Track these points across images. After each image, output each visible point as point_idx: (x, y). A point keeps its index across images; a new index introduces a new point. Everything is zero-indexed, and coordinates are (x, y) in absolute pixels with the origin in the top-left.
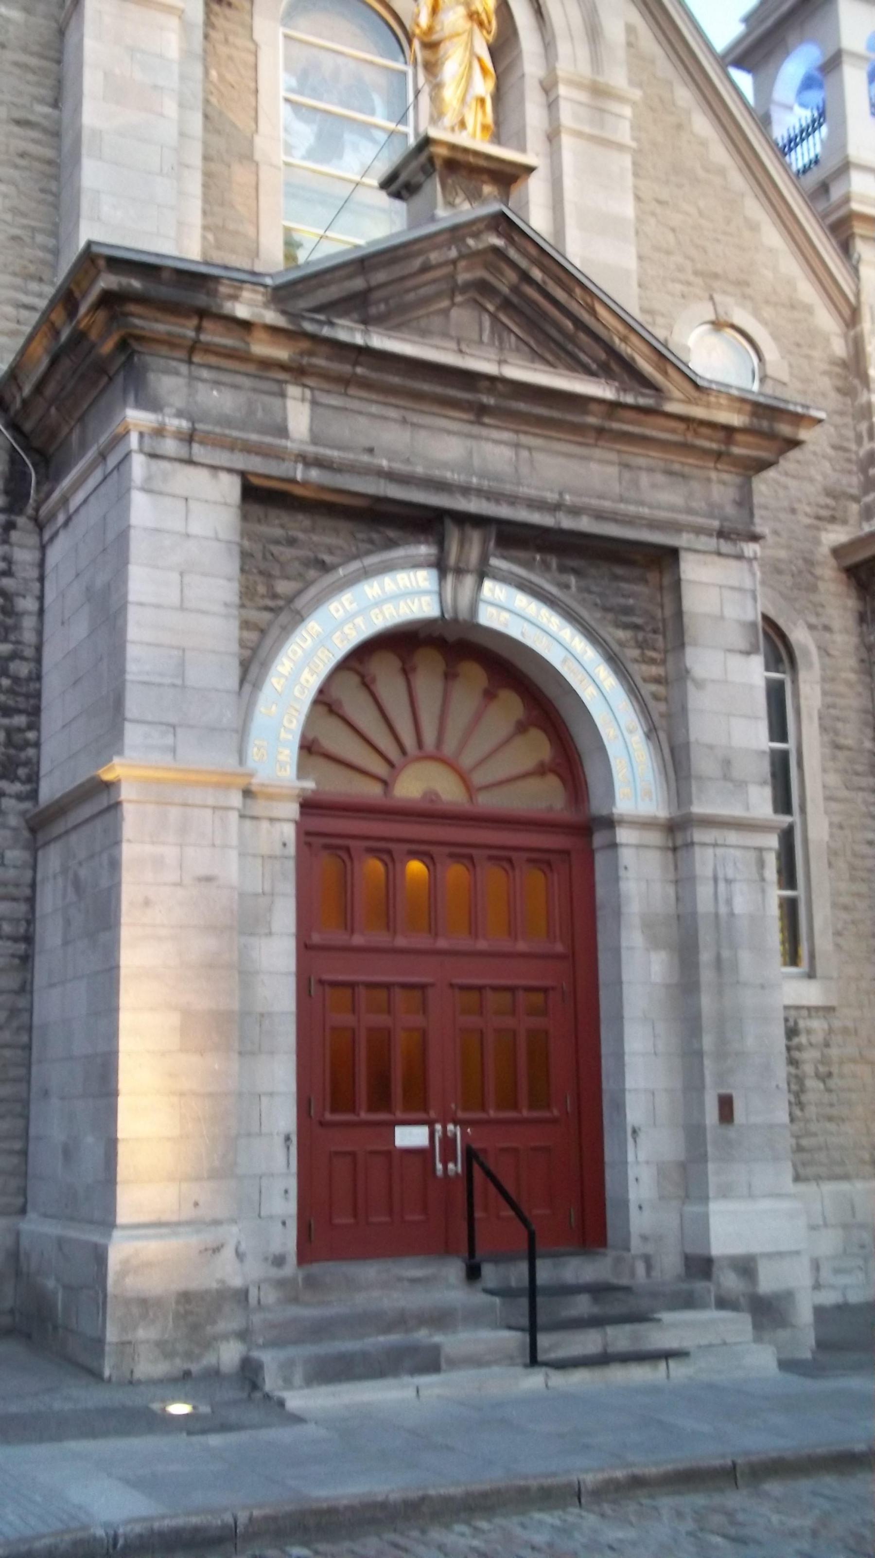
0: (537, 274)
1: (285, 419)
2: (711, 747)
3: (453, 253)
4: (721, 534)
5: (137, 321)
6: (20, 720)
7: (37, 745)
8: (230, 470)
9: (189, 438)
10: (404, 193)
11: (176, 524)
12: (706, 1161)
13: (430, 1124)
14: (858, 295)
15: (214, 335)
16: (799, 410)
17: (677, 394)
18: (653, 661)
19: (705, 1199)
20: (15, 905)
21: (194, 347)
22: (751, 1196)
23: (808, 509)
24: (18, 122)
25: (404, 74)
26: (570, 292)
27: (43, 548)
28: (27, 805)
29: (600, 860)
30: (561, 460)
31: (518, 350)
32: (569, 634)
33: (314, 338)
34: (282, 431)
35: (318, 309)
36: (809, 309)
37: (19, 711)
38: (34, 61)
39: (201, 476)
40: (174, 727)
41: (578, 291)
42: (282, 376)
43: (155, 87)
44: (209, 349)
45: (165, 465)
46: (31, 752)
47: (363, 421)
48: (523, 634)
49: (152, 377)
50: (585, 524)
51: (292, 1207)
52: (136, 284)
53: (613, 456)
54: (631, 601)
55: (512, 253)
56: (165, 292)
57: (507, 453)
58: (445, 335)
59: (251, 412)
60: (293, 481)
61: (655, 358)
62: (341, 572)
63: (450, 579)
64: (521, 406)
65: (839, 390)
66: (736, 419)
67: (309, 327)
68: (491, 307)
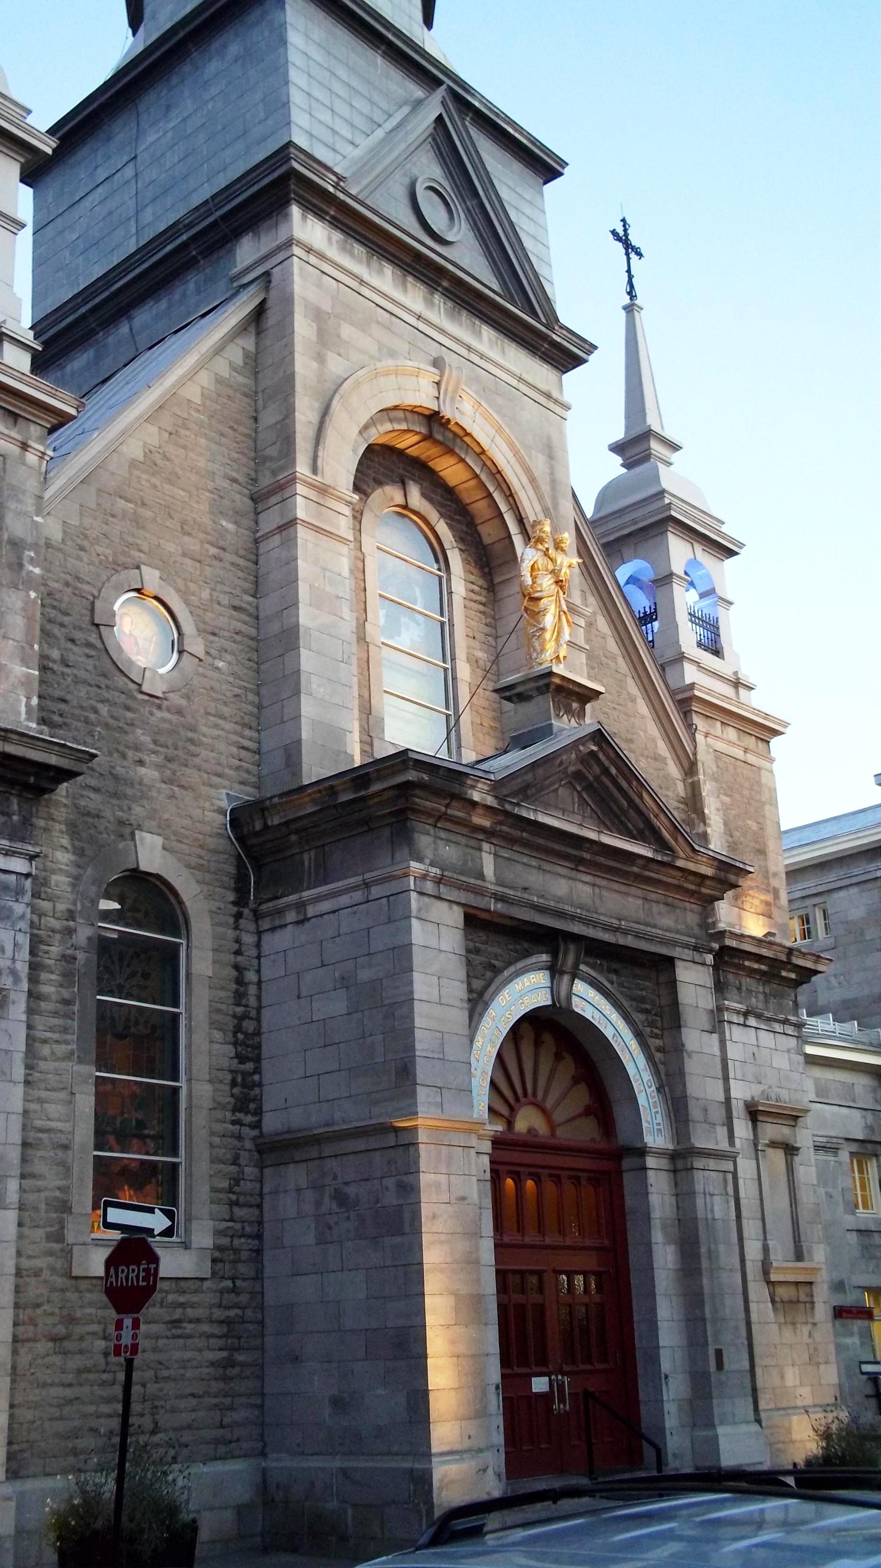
0: (613, 771)
2: (697, 1099)
4: (696, 949)
5: (417, 800)
6: (249, 1066)
7: (260, 1085)
8: (458, 904)
10: (515, 699)
11: (433, 943)
12: (712, 1398)
13: (548, 1374)
14: (695, 754)
15: (456, 812)
16: (741, 866)
17: (682, 854)
19: (712, 1426)
20: (251, 1210)
21: (442, 817)
22: (735, 1423)
24: (235, 608)
25: (440, 578)
26: (630, 784)
27: (259, 933)
28: (256, 1133)
29: (628, 1179)
30: (615, 896)
31: (591, 818)
32: (615, 1017)
33: (507, 814)
36: (664, 760)
37: (249, 1059)
38: (241, 562)
39: (443, 906)
40: (440, 1088)
41: (634, 783)
42: (481, 836)
43: (338, 597)
45: (426, 899)
46: (257, 1091)
47: (519, 867)
49: (416, 835)
50: (629, 941)
52: (426, 777)
53: (639, 892)
54: (644, 993)
55: (601, 756)
56: (439, 783)
57: (588, 889)
58: (557, 807)
59: (466, 862)
60: (488, 911)
61: (672, 829)
64: (601, 860)
66: (709, 871)
67: (508, 807)
68: (579, 788)
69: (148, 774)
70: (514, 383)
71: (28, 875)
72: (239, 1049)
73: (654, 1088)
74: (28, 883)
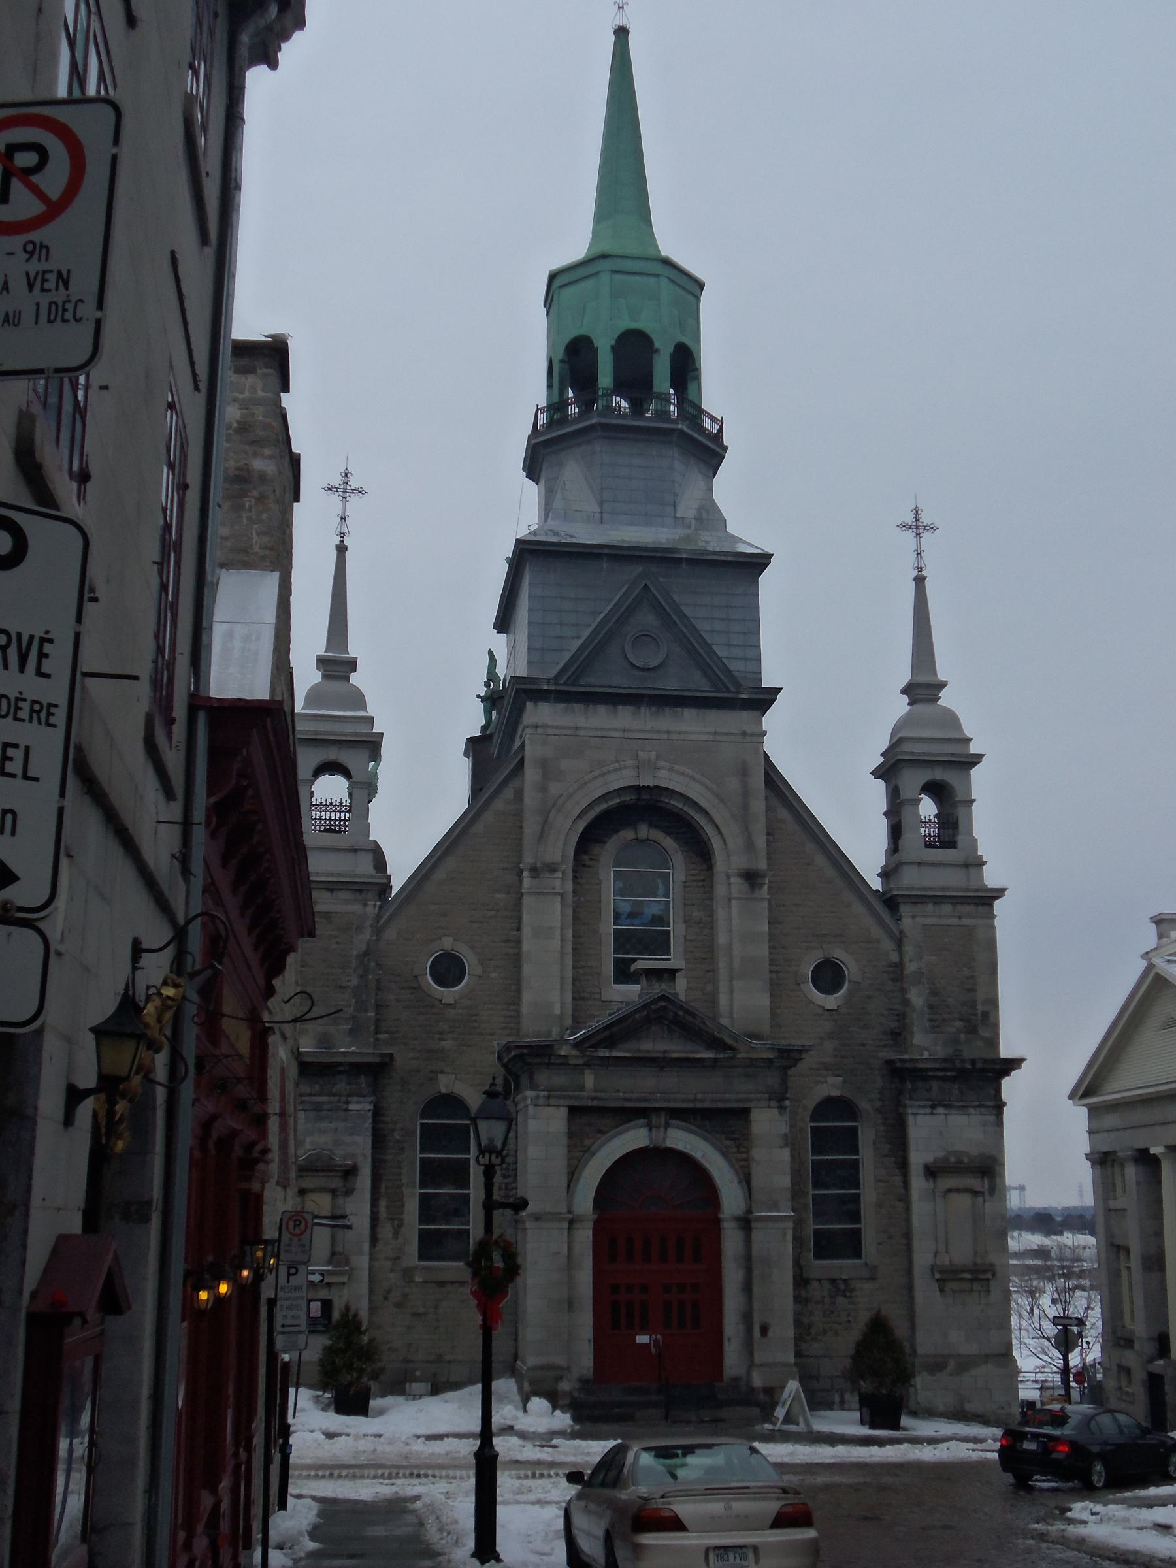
1: (584, 1083)
3: (645, 1013)
6: (510, 1180)
8: (563, 1106)
9: (549, 1097)
18: (742, 1152)
23: (872, 1043)
24: (507, 941)
34: (582, 1088)
35: (589, 1047)
36: (878, 941)
43: (551, 928)
44: (554, 1064)
46: (514, 1191)
48: (685, 1148)
50: (707, 1105)
51: (592, 1364)
52: (525, 1051)
55: (670, 1007)
62: (608, 1135)
63: (654, 1130)
65: (893, 980)
66: (771, 1056)
67: (588, 1053)
68: (666, 1022)
69: (447, 1044)
70: (710, 738)
71: (369, 1110)
72: (504, 1171)
73: (736, 1182)
74: (370, 1114)
